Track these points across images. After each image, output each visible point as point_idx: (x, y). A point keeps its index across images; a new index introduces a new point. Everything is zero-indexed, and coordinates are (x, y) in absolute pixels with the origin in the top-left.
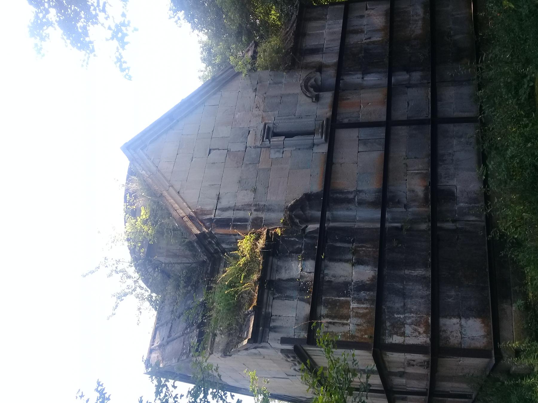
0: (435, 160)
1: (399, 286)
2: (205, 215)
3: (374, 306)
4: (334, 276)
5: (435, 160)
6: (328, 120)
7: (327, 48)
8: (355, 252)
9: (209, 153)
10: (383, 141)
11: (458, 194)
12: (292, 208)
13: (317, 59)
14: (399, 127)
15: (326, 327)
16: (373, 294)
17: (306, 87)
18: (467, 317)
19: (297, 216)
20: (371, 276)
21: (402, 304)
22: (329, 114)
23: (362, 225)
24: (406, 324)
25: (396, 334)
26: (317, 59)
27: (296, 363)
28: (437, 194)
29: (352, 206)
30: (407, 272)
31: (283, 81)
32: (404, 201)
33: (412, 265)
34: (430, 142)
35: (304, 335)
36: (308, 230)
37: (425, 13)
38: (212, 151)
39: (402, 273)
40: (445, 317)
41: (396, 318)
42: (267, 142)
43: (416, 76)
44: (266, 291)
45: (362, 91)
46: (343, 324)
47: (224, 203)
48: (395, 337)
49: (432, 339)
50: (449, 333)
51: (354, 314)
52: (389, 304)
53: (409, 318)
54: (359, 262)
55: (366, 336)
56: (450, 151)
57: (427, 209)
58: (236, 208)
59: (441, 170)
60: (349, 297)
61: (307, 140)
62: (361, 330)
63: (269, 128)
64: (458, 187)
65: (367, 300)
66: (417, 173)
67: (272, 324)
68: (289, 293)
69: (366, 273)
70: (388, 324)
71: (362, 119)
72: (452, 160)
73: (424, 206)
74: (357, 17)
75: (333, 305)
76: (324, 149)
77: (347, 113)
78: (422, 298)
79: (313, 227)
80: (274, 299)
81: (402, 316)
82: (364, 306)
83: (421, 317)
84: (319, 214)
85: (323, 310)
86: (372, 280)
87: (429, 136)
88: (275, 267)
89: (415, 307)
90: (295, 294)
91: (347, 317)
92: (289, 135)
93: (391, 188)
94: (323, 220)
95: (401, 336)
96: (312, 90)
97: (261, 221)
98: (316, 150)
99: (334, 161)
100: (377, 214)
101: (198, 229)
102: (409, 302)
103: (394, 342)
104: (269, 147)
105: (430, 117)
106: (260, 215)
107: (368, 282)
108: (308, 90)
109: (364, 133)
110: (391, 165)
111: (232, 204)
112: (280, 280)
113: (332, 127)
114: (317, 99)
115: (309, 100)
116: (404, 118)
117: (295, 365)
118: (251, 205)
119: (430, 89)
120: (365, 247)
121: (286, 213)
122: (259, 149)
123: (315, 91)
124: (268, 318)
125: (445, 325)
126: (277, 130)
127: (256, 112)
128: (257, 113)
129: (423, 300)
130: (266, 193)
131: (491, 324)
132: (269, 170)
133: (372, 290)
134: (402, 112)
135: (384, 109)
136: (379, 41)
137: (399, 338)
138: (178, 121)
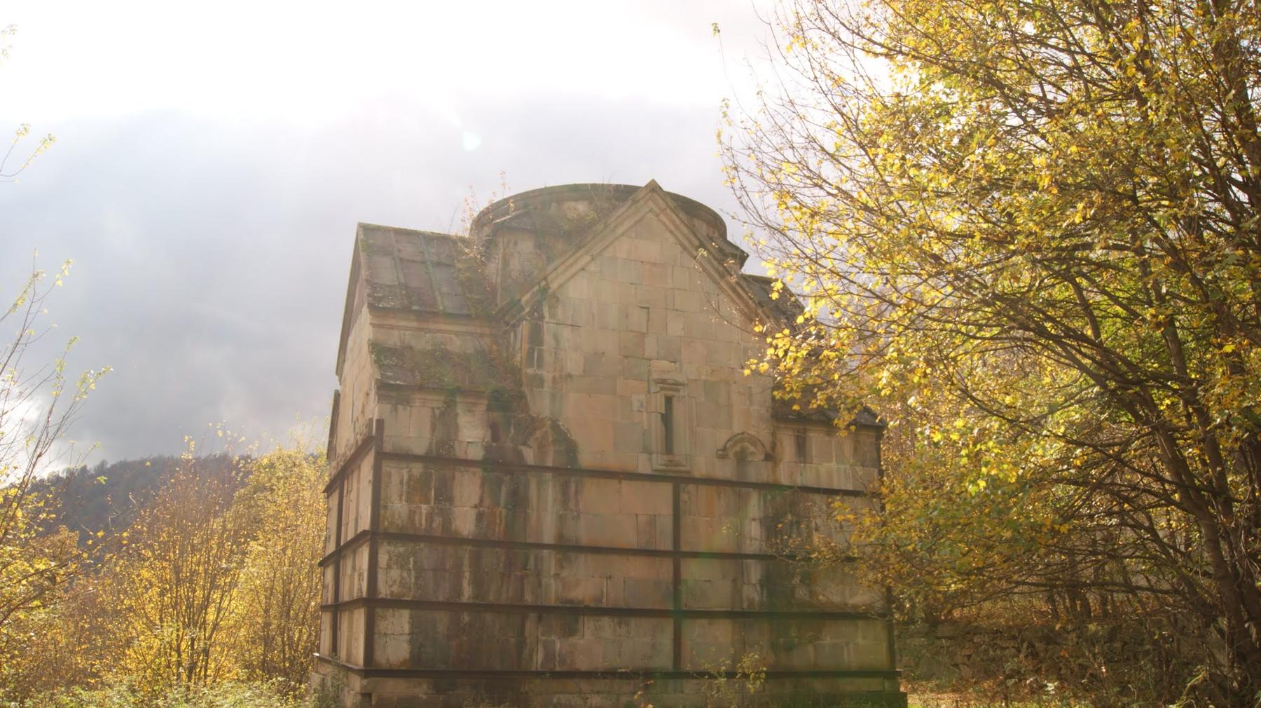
0: (621, 613)
3: (422, 533)
5: (621, 613)
6: (688, 472)
10: (652, 548)
11: (571, 640)
12: (555, 426)
14: (671, 568)
15: (397, 475)
16: (438, 533)
18: (411, 642)
22: (697, 475)
25: (390, 559)
30: (467, 575)
32: (565, 573)
33: (477, 582)
35: (388, 447)
37: (855, 607)
43: (752, 593)
44: (443, 398)
46: (401, 496)
47: (566, 333)
53: (409, 576)
54: (480, 517)
59: (606, 622)
67: (400, 407)
69: (465, 523)
70: (402, 549)
71: (686, 520)
76: (644, 468)
77: (696, 497)
79: (530, 456)
82: (424, 522)
84: (550, 463)
85: (417, 469)
91: (408, 500)
92: (667, 419)
93: (582, 557)
94: (540, 469)
96: (738, 448)
98: (643, 457)
101: (527, 302)
104: (649, 392)
110: (615, 558)
112: (457, 415)
113: (679, 480)
115: (721, 445)
124: (407, 402)
126: (675, 403)
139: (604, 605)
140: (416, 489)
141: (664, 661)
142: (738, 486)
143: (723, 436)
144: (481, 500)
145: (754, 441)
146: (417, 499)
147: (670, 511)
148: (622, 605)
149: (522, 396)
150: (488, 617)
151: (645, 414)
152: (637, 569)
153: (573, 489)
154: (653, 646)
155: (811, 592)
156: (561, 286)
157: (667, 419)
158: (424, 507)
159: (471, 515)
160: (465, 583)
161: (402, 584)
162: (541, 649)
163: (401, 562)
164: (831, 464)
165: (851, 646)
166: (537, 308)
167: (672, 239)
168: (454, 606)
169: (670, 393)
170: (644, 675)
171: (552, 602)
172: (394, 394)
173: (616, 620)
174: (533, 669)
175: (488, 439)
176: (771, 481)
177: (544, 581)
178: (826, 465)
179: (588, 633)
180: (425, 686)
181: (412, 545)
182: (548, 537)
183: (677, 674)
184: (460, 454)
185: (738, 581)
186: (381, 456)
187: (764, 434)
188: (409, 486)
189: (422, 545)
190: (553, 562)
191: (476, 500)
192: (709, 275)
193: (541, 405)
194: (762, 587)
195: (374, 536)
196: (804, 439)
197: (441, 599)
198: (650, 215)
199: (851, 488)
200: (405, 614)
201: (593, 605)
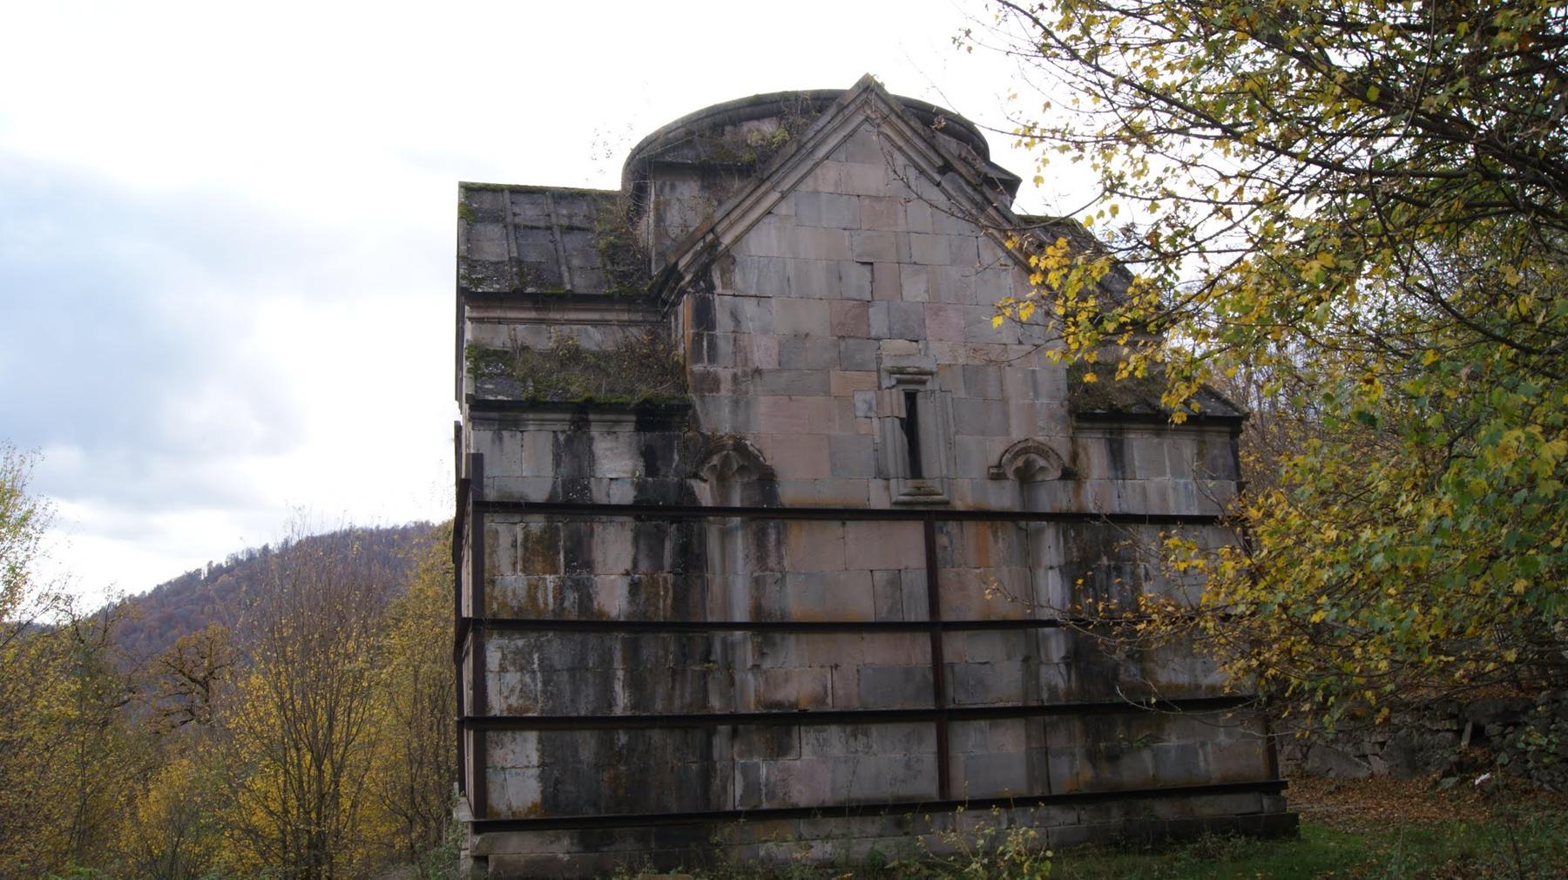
0: (855, 719)
5: (855, 719)
6: (947, 503)
10: (898, 619)
11: (784, 762)
12: (740, 447)
14: (929, 649)
16: (573, 617)
17: (1025, 449)
18: (542, 778)
22: (960, 505)
25: (504, 657)
28: (781, 724)
30: (620, 674)
31: (1044, 400)
32: (767, 664)
33: (636, 683)
34: (896, 708)
35: (491, 495)
37: (1213, 688)
40: (540, 741)
41: (531, 654)
42: (887, 382)
43: (1056, 678)
46: (514, 564)
47: (749, 308)
49: (495, 719)
52: (556, 644)
53: (534, 680)
54: (634, 588)
55: (495, 606)
59: (834, 733)
62: (505, 596)
63: (924, 382)
64: (798, 763)
67: (506, 434)
68: (566, 459)
69: (613, 599)
70: (520, 643)
71: (947, 574)
76: (879, 501)
77: (960, 541)
78: (572, 701)
79: (705, 493)
82: (551, 600)
84: (736, 502)
85: (537, 523)
86: (601, 613)
87: (909, 707)
92: (910, 425)
93: (792, 640)
94: (724, 511)
96: (1020, 462)
97: (711, 391)
98: (876, 485)
99: (849, 523)
100: (741, 614)
101: (688, 266)
103: (488, 654)
104: (880, 388)
108: (1017, 455)
109: (917, 581)
110: (843, 638)
111: (748, 325)
112: (591, 439)
113: (932, 515)
114: (997, 475)
115: (994, 460)
116: (949, 655)
120: (666, 593)
122: (873, 366)
123: (1017, 471)
124: (516, 425)
125: (525, 740)
126: (920, 401)
130: (774, 393)
131: (532, 817)
132: (827, 393)
135: (972, 616)
137: (497, 662)
138: (938, 185)
139: (829, 709)
140: (536, 553)
141: (926, 787)
142: (1020, 518)
143: (996, 448)
145: (1042, 451)
146: (539, 567)
147: (924, 565)
148: (856, 706)
149: (688, 406)
150: (656, 736)
151: (875, 421)
152: (876, 652)
153: (773, 538)
154: (908, 766)
155: (1143, 670)
157: (910, 425)
158: (550, 578)
159: (622, 587)
160: (618, 687)
161: (524, 692)
162: (738, 777)
164: (1163, 477)
165: (1209, 748)
166: (703, 273)
168: (602, 723)
169: (912, 386)
170: (900, 811)
171: (752, 708)
172: (494, 415)
173: (849, 729)
174: (729, 807)
175: (640, 471)
176: (1074, 509)
177: (737, 677)
179: (806, 750)
180: (566, 842)
181: (535, 635)
182: (741, 614)
183: (945, 805)
184: (599, 497)
185: (1031, 662)
187: (1059, 441)
188: (526, 548)
189: (550, 634)
190: (749, 646)
191: (628, 565)
193: (718, 418)
194: (1068, 665)
196: (1121, 443)
197: (583, 713)
198: (867, 126)
199: (1195, 511)
200: (532, 737)
201: (811, 709)
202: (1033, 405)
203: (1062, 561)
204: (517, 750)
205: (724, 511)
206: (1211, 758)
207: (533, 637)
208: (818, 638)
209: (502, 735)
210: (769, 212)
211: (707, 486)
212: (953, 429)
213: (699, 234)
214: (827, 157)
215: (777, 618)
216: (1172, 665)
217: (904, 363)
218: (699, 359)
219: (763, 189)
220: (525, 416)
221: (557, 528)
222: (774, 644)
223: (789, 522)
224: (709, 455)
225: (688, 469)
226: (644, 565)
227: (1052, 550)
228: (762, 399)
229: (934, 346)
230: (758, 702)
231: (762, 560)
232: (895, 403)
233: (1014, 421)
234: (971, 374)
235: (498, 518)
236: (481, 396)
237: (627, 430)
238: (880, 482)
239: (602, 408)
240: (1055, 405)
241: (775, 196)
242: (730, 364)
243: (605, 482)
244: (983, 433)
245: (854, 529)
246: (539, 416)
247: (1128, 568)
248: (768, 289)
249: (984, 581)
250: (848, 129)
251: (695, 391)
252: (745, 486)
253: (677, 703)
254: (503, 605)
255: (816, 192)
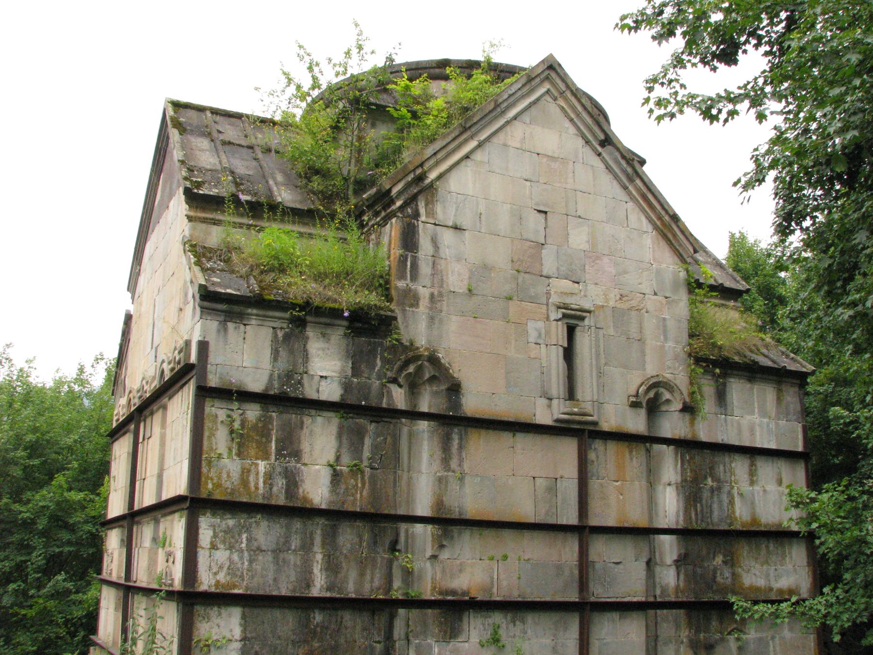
1: (295, 542)
2: (426, 205)
3: (260, 500)
4: (311, 433)
6: (595, 424)
7: (726, 420)
8: (356, 470)
9: (540, 211)
10: (552, 521)
12: (433, 360)
13: (708, 405)
16: (281, 501)
19: (420, 369)
20: (311, 496)
21: (264, 548)
22: (605, 427)
23: (404, 482)
24: (231, 553)
25: (215, 536)
26: (708, 405)
27: (172, 365)
29: (437, 466)
30: (319, 557)
31: (670, 344)
32: (445, 555)
33: (332, 567)
34: (548, 599)
35: (213, 381)
36: (394, 388)
38: (543, 215)
39: (317, 548)
40: (244, 617)
41: (240, 535)
42: (555, 315)
43: (669, 578)
45: (644, 483)
47: (447, 237)
48: (211, 533)
50: (218, 621)
51: (247, 466)
53: (241, 558)
54: (336, 477)
55: (210, 486)
56: (529, 631)
57: (429, 592)
58: (437, 261)
60: (276, 459)
61: (557, 387)
62: (219, 478)
63: (582, 319)
64: (466, 644)
65: (271, 489)
66: (492, 578)
67: (231, 326)
68: (283, 354)
70: (231, 522)
71: (594, 485)
72: (514, 636)
73: (435, 588)
74: (780, 474)
75: (263, 430)
76: (544, 417)
77: (605, 456)
78: (275, 580)
79: (399, 397)
80: (274, 328)
81: (244, 545)
82: (261, 484)
83: (242, 576)
84: (424, 408)
85: (253, 412)
86: (305, 499)
88: (329, 331)
89: (259, 568)
90: (283, 364)
92: (569, 354)
95: (212, 543)
96: (651, 394)
97: (412, 306)
100: (423, 508)
101: (400, 193)
102: (270, 557)
103: (201, 531)
104: (548, 318)
105: (592, 599)
106: (424, 303)
107: (301, 491)
109: (570, 489)
110: (507, 533)
112: (308, 338)
113: (582, 432)
114: (635, 405)
115: (632, 391)
116: (593, 555)
117: (169, 363)
118: (442, 286)
119: (643, 599)
121: (427, 349)
122: (544, 301)
123: (649, 401)
124: (240, 318)
125: (230, 615)
127: (614, 295)
128: (612, 295)
129: (271, 582)
130: (463, 314)
133: (287, 498)
134: (603, 551)
135: (611, 522)
136: (734, 512)
138: (599, 155)
144: (338, 458)
145: (669, 386)
146: (252, 452)
147: (575, 474)
148: (515, 596)
150: (347, 617)
152: (535, 549)
153: (455, 443)
155: (733, 574)
156: (440, 177)
157: (569, 354)
160: (317, 570)
163: (229, 540)
165: (777, 640)
167: (572, 130)
169: (572, 321)
172: (224, 307)
173: (509, 616)
176: (689, 437)
178: (748, 417)
181: (245, 516)
184: (311, 393)
186: (204, 393)
189: (259, 516)
191: (331, 457)
192: (616, 177)
193: (416, 329)
195: (194, 504)
196: (724, 385)
197: (284, 592)
199: (773, 446)
202: (662, 347)
203: (679, 480)
204: (222, 624)
205: (415, 415)
206: (778, 648)
207: (243, 519)
208: (488, 533)
209: (208, 610)
210: (467, 157)
211: (399, 390)
212: (603, 361)
213: (411, 167)
214: (515, 118)
215: (456, 516)
216: (753, 571)
217: (568, 300)
218: (402, 277)
219: (465, 136)
220: (250, 311)
221: (271, 416)
222: (452, 537)
223: (469, 429)
224: (407, 363)
225: (389, 374)
226: (346, 459)
227: (671, 469)
228: (454, 318)
229: (591, 287)
230: (434, 588)
231: (446, 461)
232: (559, 333)
233: (648, 358)
234: (619, 315)
235: (218, 403)
236: (211, 288)
237: (337, 335)
238: (544, 401)
239: (318, 311)
240: (679, 349)
241: (473, 144)
242: (429, 284)
243: (317, 378)
244: (625, 367)
245: (523, 441)
246: (261, 312)
247: (726, 489)
248: (465, 222)
249: (621, 493)
250: (533, 98)
251: (398, 304)
252: (435, 394)
253: (367, 587)
254: (218, 485)
255: (505, 145)
